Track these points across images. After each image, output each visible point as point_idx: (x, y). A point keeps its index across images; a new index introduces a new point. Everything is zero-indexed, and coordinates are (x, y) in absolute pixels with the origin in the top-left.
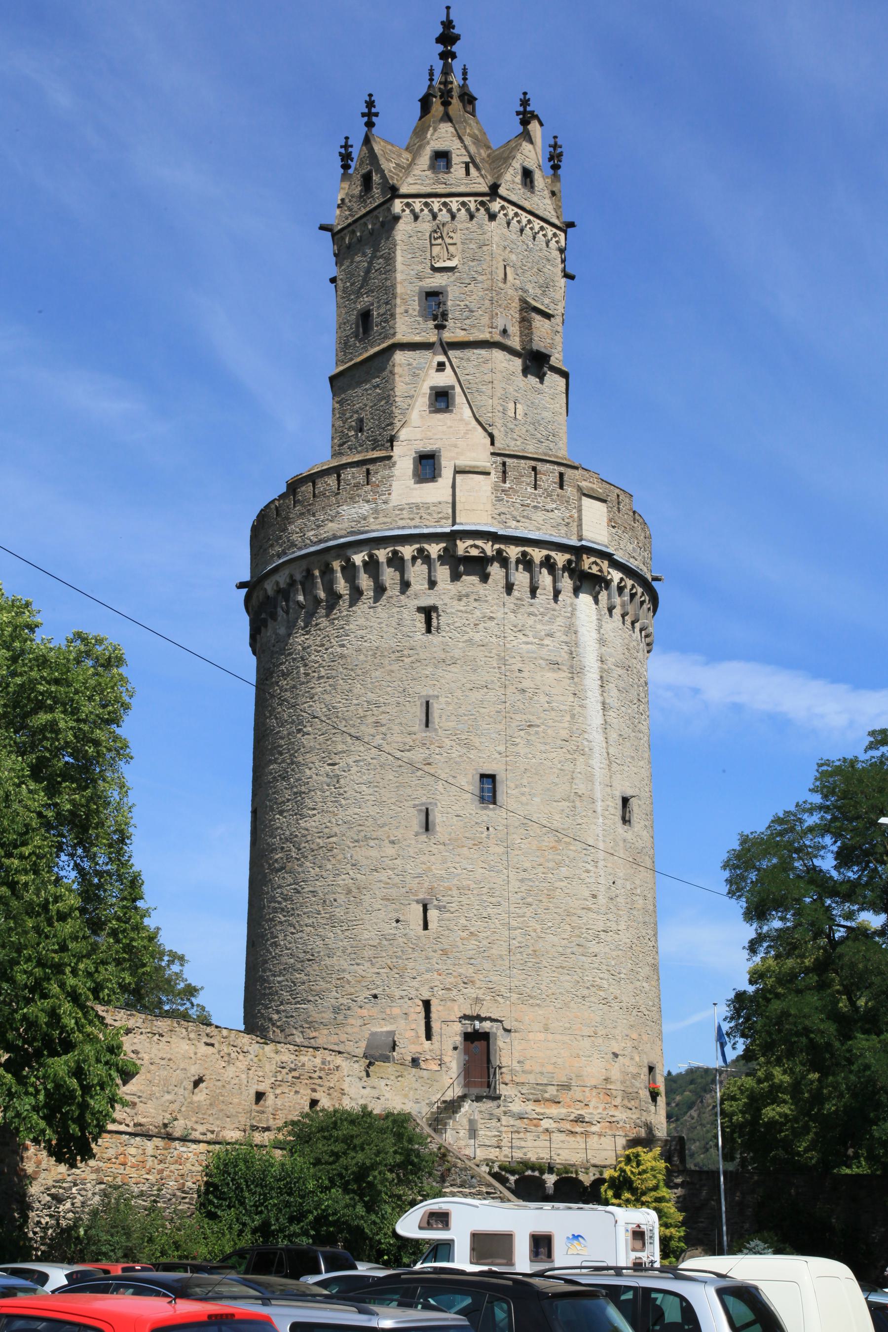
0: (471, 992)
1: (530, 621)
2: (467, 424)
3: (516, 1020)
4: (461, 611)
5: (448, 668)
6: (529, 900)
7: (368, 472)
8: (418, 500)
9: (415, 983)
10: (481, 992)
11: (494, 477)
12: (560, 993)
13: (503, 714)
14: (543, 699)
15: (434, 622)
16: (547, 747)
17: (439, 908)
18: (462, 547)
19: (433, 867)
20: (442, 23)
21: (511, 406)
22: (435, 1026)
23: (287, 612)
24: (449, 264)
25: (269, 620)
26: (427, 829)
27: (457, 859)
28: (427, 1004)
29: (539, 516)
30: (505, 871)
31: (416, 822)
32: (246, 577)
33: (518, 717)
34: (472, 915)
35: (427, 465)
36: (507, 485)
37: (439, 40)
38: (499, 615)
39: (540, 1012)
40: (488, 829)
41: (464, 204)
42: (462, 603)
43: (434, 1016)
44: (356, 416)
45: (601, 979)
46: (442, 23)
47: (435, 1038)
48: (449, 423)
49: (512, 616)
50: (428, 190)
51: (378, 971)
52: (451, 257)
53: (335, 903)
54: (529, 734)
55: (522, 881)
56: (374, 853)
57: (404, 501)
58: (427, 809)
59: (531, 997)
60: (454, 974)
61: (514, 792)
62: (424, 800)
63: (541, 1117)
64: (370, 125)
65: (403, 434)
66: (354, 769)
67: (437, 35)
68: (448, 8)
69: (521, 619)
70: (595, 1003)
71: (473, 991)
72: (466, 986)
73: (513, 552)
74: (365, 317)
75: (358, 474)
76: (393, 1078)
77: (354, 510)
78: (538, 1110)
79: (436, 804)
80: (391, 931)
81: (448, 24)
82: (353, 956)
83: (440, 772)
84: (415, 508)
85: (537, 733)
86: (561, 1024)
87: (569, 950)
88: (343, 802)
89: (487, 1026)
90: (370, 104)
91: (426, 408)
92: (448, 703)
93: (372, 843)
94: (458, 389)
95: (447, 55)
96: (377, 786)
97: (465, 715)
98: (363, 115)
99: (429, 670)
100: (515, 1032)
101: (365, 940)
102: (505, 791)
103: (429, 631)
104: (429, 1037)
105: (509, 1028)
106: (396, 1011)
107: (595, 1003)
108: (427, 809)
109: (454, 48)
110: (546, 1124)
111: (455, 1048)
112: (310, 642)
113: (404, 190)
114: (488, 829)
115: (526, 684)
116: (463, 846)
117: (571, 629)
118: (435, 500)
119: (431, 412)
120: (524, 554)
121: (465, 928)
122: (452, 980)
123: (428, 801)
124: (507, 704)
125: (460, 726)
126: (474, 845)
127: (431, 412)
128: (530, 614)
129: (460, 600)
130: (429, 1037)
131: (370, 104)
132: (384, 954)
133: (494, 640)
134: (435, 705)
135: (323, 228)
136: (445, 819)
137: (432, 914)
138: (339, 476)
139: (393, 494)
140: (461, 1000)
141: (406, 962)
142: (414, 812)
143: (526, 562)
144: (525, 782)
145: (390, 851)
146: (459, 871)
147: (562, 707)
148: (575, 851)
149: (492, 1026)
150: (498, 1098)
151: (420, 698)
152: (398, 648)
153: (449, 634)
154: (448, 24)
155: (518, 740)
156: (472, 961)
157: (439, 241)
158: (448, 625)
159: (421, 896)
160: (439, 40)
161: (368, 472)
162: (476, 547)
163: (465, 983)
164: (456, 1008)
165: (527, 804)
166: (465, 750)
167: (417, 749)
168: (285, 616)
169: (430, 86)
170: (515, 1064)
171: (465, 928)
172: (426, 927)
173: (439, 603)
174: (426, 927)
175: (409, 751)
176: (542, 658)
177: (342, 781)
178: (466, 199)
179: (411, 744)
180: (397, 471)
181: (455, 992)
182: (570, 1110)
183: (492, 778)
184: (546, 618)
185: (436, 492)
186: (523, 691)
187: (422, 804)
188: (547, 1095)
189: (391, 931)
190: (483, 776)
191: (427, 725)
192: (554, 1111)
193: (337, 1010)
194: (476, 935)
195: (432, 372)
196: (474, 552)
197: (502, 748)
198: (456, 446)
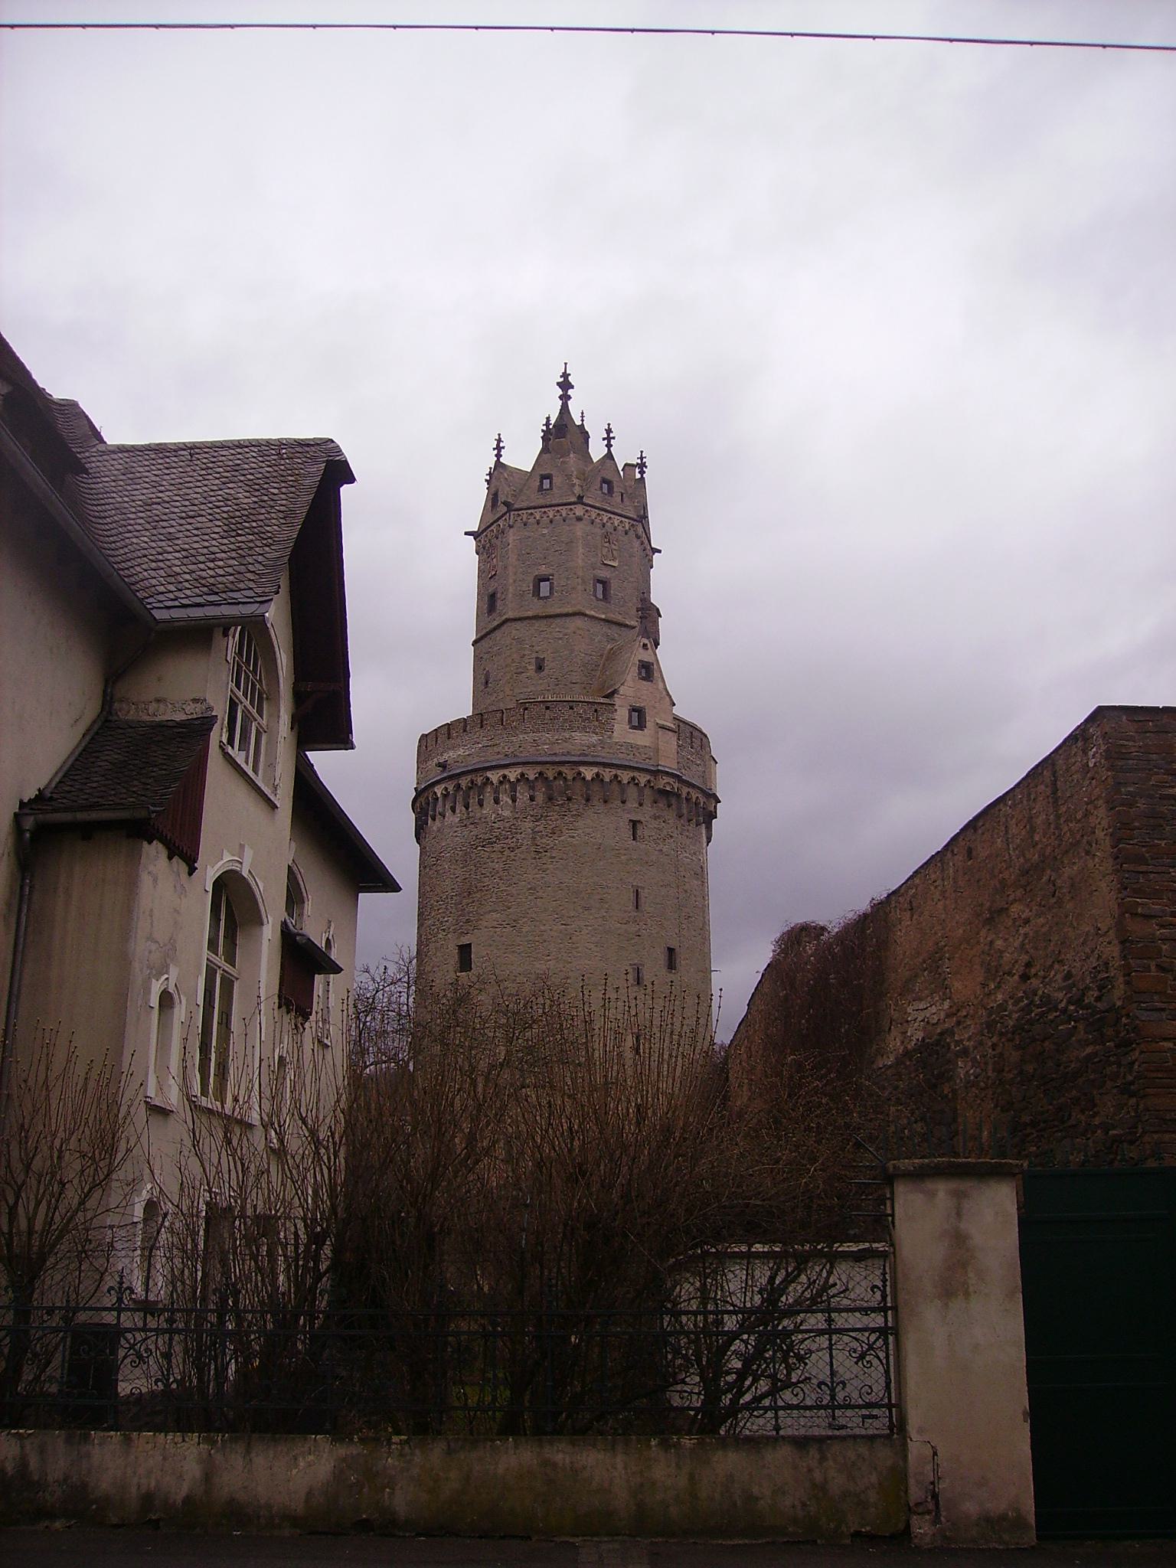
1: (688, 841)
15: (639, 833)
29: (694, 768)
44: (534, 655)
66: (585, 931)
73: (685, 790)
81: (565, 375)
102: (681, 962)
112: (541, 828)
154: (565, 375)
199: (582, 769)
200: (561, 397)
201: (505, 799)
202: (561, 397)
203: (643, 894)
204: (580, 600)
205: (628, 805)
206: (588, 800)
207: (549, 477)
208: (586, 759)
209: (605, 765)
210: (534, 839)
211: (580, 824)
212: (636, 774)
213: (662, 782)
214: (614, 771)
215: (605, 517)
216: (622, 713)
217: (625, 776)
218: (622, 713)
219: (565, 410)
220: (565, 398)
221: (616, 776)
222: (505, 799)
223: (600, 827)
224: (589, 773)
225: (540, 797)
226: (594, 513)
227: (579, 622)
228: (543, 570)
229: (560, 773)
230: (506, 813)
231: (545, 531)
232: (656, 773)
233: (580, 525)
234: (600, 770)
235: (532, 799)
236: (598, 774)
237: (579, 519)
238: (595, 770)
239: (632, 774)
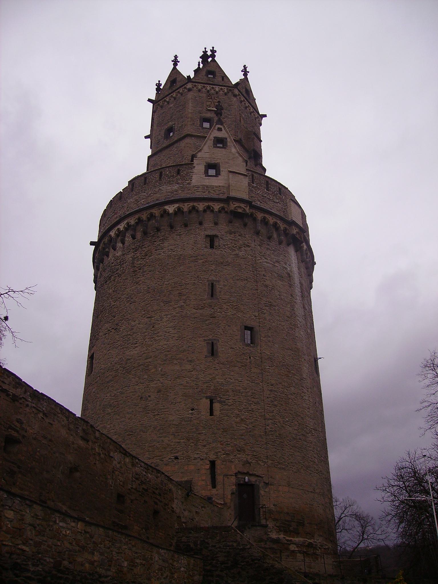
2: (233, 154)
3: (271, 477)
4: (232, 240)
5: (225, 267)
6: (276, 403)
7: (179, 170)
8: (208, 184)
10: (249, 457)
12: (295, 463)
13: (257, 296)
15: (216, 244)
16: (280, 318)
17: (220, 402)
19: (217, 377)
20: (203, 52)
22: (219, 478)
23: (123, 243)
25: (112, 250)
26: (213, 354)
27: (232, 373)
28: (213, 464)
30: (261, 384)
31: (205, 350)
32: (96, 240)
33: (264, 299)
34: (242, 408)
38: (253, 245)
39: (285, 474)
40: (250, 357)
41: (221, 89)
42: (232, 236)
43: (218, 471)
45: (315, 457)
46: (203, 52)
47: (219, 486)
48: (224, 153)
49: (259, 247)
51: (179, 441)
53: (149, 398)
54: (271, 309)
55: (271, 391)
56: (177, 368)
57: (199, 184)
58: (213, 343)
59: (279, 464)
60: (232, 444)
61: (264, 339)
62: (210, 337)
63: (289, 543)
65: (199, 155)
66: (165, 319)
67: (201, 55)
68: (205, 48)
70: (313, 472)
71: (244, 456)
72: (239, 453)
73: (260, 216)
76: (200, 507)
77: (169, 188)
78: (287, 538)
79: (218, 340)
80: (188, 416)
82: (161, 431)
83: (221, 322)
85: (275, 309)
86: (297, 482)
87: (298, 437)
88: (157, 338)
89: (253, 479)
92: (225, 286)
93: (175, 362)
94: (228, 140)
96: (179, 329)
97: (234, 292)
99: (214, 267)
100: (271, 485)
101: (170, 421)
104: (214, 486)
105: (267, 482)
106: (192, 467)
107: (313, 472)
108: (213, 343)
110: (293, 547)
112: (138, 255)
114: (250, 357)
115: (268, 283)
116: (235, 366)
118: (216, 185)
119: (214, 147)
120: (264, 218)
121: (238, 416)
122: (230, 448)
123: (214, 338)
124: (259, 291)
125: (232, 299)
126: (242, 366)
127: (214, 147)
128: (268, 249)
129: (231, 234)
130: (214, 486)
132: (183, 430)
133: (250, 257)
134: (217, 286)
136: (223, 349)
137: (217, 406)
139: (193, 181)
140: (237, 462)
141: (199, 436)
143: (265, 222)
144: (270, 334)
145: (188, 367)
146: (233, 381)
147: (286, 300)
148: (297, 379)
149: (256, 481)
151: (208, 281)
152: (194, 255)
153: (225, 250)
155: (265, 311)
156: (243, 437)
157: (211, 100)
158: (224, 245)
159: (209, 395)
161: (179, 170)
162: (240, 207)
163: (238, 451)
164: (233, 467)
165: (272, 347)
166: (235, 312)
167: (206, 308)
168: (121, 245)
170: (272, 506)
171: (238, 416)
172: (211, 414)
173: (219, 234)
174: (211, 414)
175: (201, 309)
176: (275, 273)
177: (156, 326)
179: (203, 305)
180: (195, 170)
182: (305, 539)
183: (251, 329)
184: (275, 253)
186: (266, 286)
187: (209, 340)
188: (291, 528)
189: (188, 416)
190: (247, 328)
191: (212, 296)
192: (296, 539)
194: (245, 421)
196: (240, 210)
197: (257, 314)
198: (228, 163)
199: (166, 207)
201: (119, 245)
203: (218, 287)
204: (189, 129)
206: (172, 227)
210: (133, 263)
211: (166, 244)
212: (211, 204)
213: (233, 206)
214: (191, 204)
217: (201, 206)
218: (199, 168)
221: (194, 207)
222: (119, 245)
224: (171, 209)
225: (139, 235)
227: (187, 140)
231: (171, 106)
233: (191, 93)
234: (181, 205)
235: (134, 237)
237: (190, 90)
238: (176, 205)
239: (207, 204)
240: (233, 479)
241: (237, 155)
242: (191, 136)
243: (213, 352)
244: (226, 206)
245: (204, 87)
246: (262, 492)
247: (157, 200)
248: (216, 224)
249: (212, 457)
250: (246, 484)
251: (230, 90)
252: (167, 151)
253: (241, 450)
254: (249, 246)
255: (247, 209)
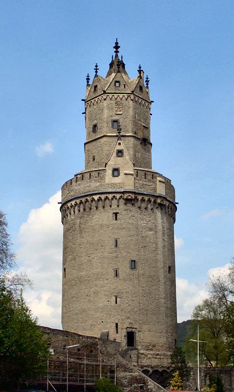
0: (129, 321)
9: (114, 319)
11: (135, 176)
14: (148, 239)
15: (118, 217)
17: (120, 298)
18: (126, 196)
21: (137, 154)
22: (119, 330)
24: (120, 113)
28: (117, 324)
31: (113, 274)
35: (116, 172)
36: (138, 178)
37: (114, 47)
50: (113, 92)
52: (120, 111)
56: (102, 282)
62: (116, 267)
64: (96, 72)
69: (142, 216)
73: (140, 197)
74: (95, 126)
75: (96, 174)
81: (117, 43)
84: (113, 185)
90: (96, 66)
91: (115, 155)
95: (117, 52)
98: (95, 69)
103: (116, 220)
104: (117, 332)
109: (119, 50)
110: (149, 356)
111: (125, 336)
113: (107, 92)
117: (155, 219)
122: (124, 317)
130: (117, 332)
131: (96, 66)
135: (83, 100)
137: (118, 299)
138: (90, 174)
142: (113, 271)
145: (107, 282)
150: (137, 349)
154: (117, 43)
160: (114, 47)
169: (112, 60)
172: (116, 303)
174: (116, 303)
178: (124, 95)
180: (107, 173)
181: (124, 321)
183: (134, 261)
185: (117, 180)
190: (132, 261)
192: (151, 352)
193: (92, 325)
195: (117, 145)
196: (129, 197)
197: (137, 253)
199: (94, 197)
200: (115, 52)
202: (115, 52)
205: (113, 207)
207: (118, 82)
208: (95, 192)
209: (87, 196)
212: (115, 195)
213: (126, 196)
215: (116, 96)
216: (109, 172)
217: (110, 196)
219: (117, 56)
220: (117, 52)
221: (107, 197)
223: (102, 217)
224: (96, 197)
225: (82, 210)
226: (111, 96)
227: (104, 139)
228: (95, 122)
229: (87, 199)
230: (73, 218)
232: (123, 193)
235: (79, 211)
236: (100, 197)
237: (105, 99)
238: (99, 196)
240: (125, 330)
241: (129, 160)
242: (107, 136)
243: (117, 275)
244: (123, 195)
245: (113, 96)
246: (137, 335)
247: (89, 191)
248: (118, 206)
249: (117, 322)
250: (130, 332)
251: (129, 96)
252: (94, 143)
253: (128, 318)
254: (134, 216)
255: (133, 196)
